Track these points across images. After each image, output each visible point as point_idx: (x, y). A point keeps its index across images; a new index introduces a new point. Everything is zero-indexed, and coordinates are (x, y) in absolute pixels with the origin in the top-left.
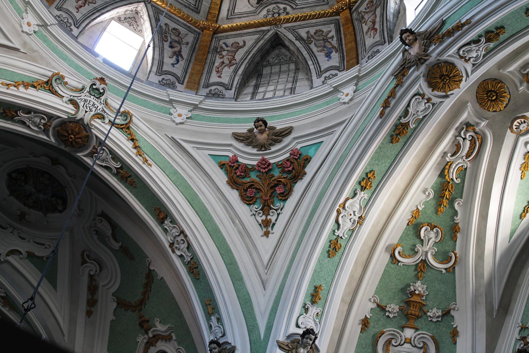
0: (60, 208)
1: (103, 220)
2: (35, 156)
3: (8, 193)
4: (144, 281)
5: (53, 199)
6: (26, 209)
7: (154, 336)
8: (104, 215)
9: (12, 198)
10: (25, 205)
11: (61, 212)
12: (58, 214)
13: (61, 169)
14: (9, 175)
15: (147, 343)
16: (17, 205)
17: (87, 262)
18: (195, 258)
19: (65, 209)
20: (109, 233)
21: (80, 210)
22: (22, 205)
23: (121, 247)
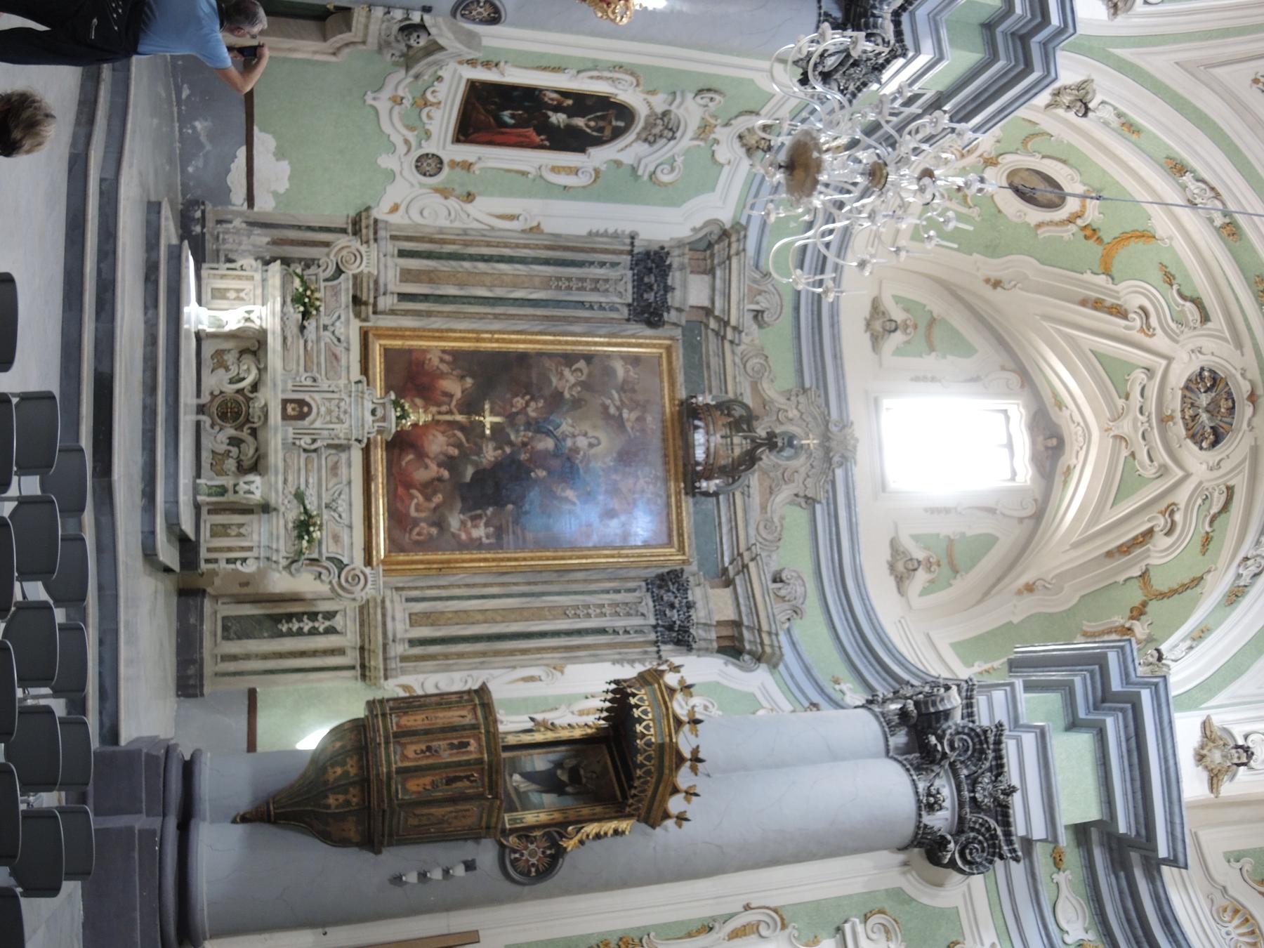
0: (1204, 445)
1: (1225, 495)
2: (1242, 375)
3: (1182, 385)
4: (1186, 581)
5: (1209, 430)
6: (1178, 415)
7: (1129, 629)
8: (1230, 490)
9: (1179, 393)
10: (1183, 411)
11: (1201, 448)
12: (1195, 448)
13: (1249, 410)
14: (1202, 369)
15: (1117, 627)
16: (1175, 403)
17: (1164, 516)
18: (1246, 589)
19: (1206, 449)
20: (1214, 510)
21: (1218, 464)
22: (1179, 409)
23: (1207, 533)
